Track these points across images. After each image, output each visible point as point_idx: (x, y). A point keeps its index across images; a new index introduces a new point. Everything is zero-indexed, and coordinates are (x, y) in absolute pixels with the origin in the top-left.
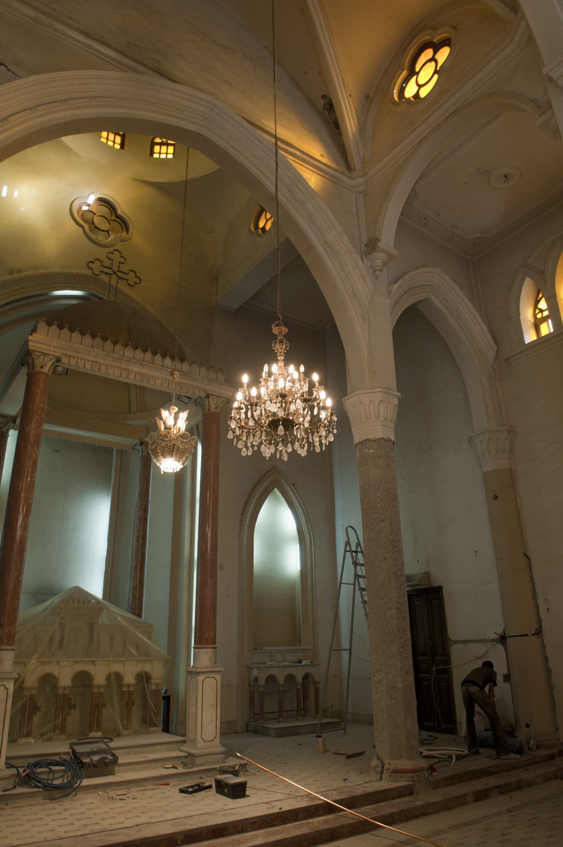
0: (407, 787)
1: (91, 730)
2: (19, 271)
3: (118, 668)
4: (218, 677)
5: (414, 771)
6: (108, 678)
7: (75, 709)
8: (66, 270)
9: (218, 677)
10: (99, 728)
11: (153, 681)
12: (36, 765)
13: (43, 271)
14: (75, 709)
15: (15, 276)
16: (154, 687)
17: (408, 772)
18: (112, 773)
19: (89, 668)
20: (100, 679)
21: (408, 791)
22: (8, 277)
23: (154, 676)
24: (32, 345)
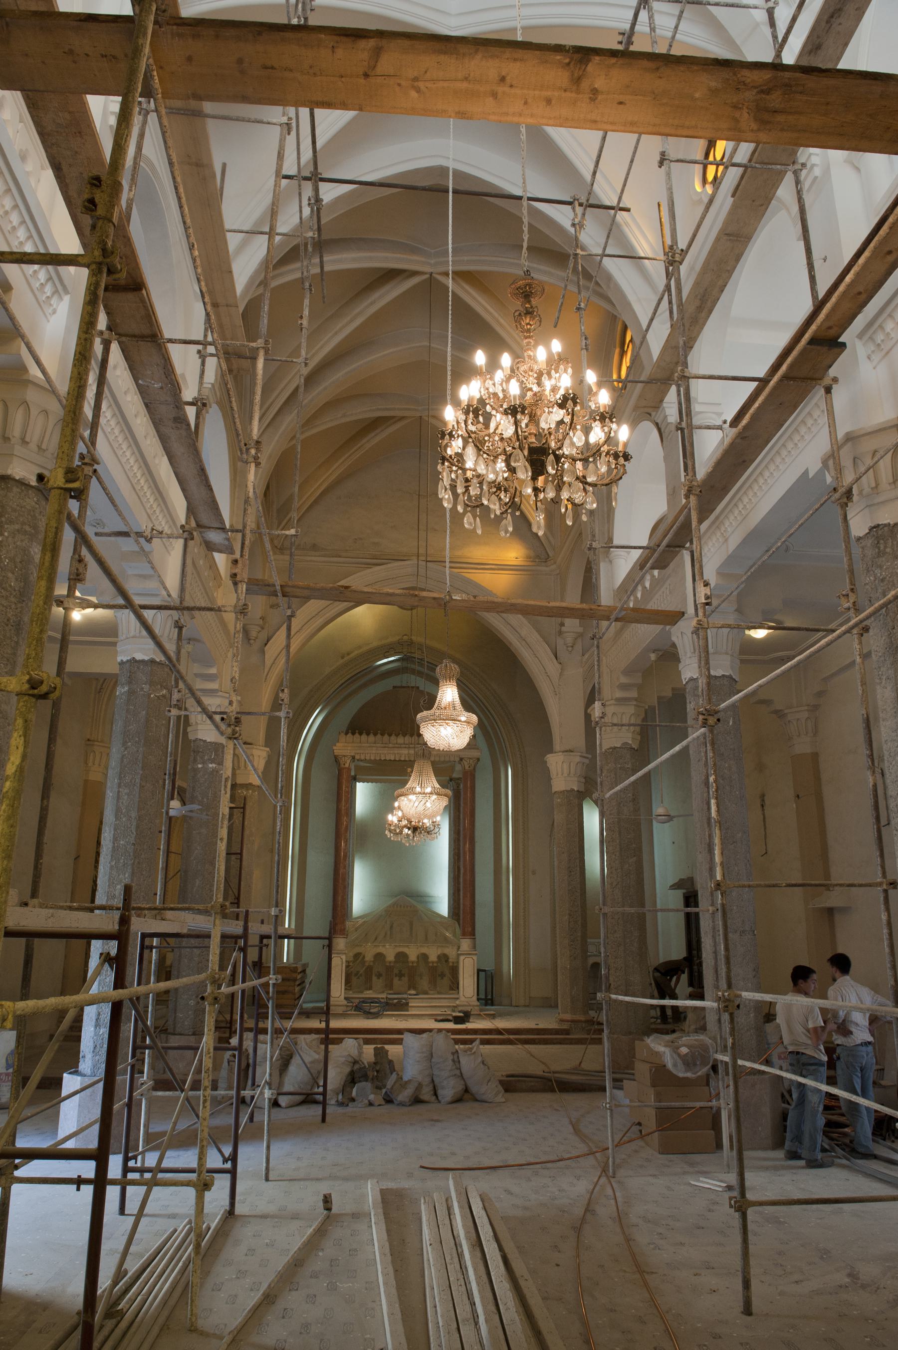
0: (564, 1030)
1: (409, 989)
2: (348, 654)
3: (424, 950)
4: (475, 958)
5: (572, 1021)
6: (439, 957)
7: (253, 962)
8: (384, 642)
9: (475, 958)
10: (414, 988)
11: (450, 960)
12: (363, 1002)
13: (365, 649)
14: (253, 962)
15: (346, 658)
16: (451, 964)
17: (568, 1021)
18: (407, 1010)
19: (406, 950)
20: (413, 957)
21: (567, 1032)
22: (341, 661)
23: (451, 957)
24: (337, 752)
